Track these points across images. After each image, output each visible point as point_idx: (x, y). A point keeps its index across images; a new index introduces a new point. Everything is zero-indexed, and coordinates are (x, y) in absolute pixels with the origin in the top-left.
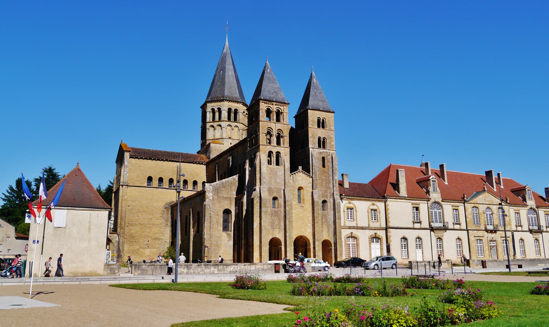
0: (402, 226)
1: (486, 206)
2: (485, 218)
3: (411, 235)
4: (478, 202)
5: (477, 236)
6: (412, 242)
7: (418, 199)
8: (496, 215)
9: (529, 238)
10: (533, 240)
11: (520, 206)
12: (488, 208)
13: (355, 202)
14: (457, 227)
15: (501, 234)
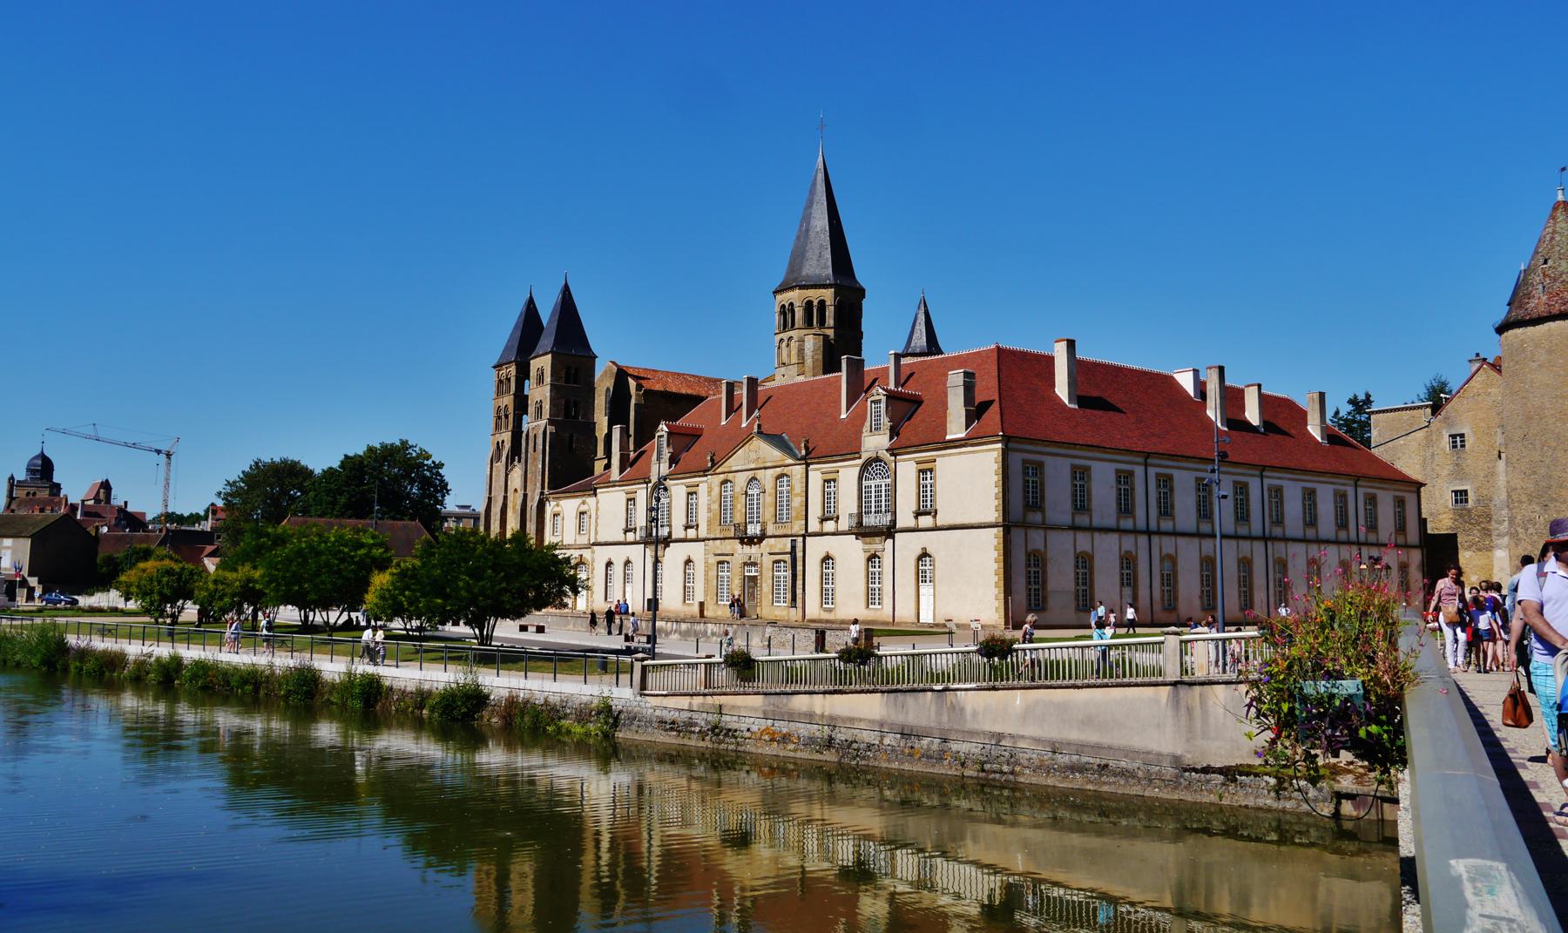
0: (610, 540)
1: (750, 474)
2: (742, 507)
3: (618, 555)
4: (734, 469)
5: (719, 552)
6: (618, 569)
7: (630, 482)
8: (770, 495)
9: (851, 552)
10: (861, 558)
11: (835, 458)
12: (754, 478)
13: (562, 502)
14: (691, 533)
15: (772, 545)
